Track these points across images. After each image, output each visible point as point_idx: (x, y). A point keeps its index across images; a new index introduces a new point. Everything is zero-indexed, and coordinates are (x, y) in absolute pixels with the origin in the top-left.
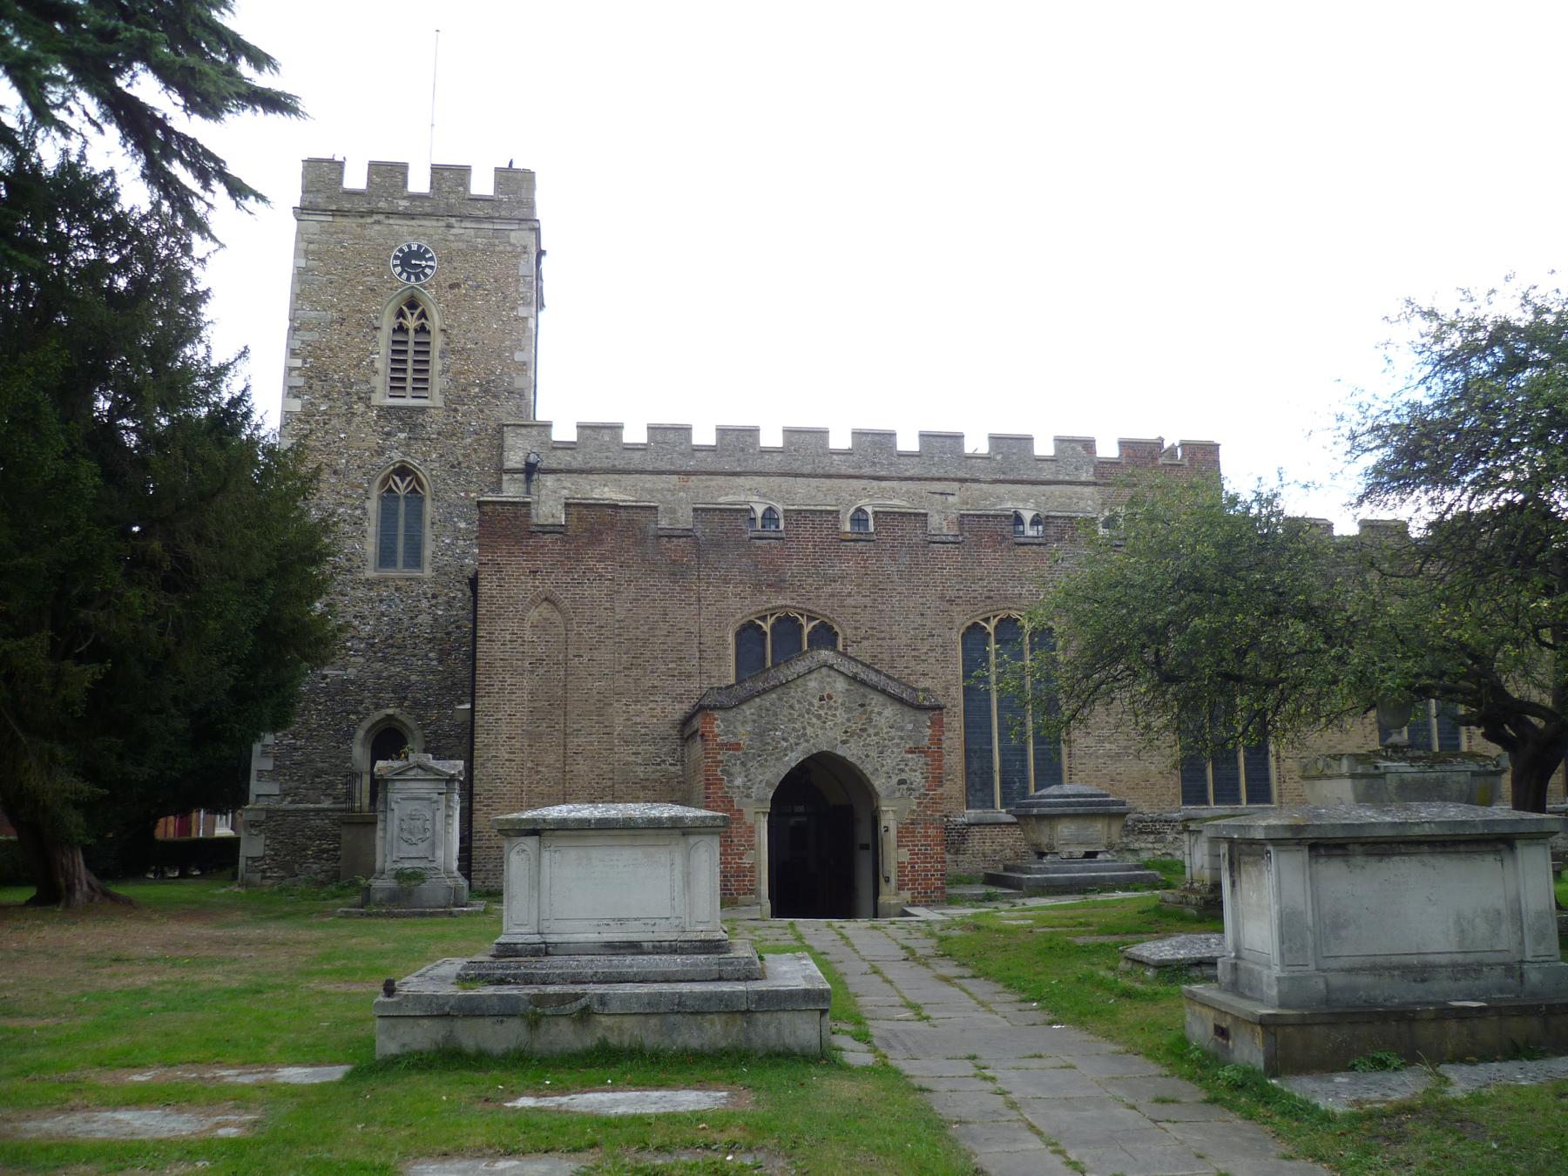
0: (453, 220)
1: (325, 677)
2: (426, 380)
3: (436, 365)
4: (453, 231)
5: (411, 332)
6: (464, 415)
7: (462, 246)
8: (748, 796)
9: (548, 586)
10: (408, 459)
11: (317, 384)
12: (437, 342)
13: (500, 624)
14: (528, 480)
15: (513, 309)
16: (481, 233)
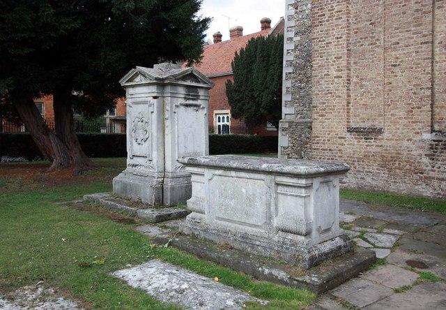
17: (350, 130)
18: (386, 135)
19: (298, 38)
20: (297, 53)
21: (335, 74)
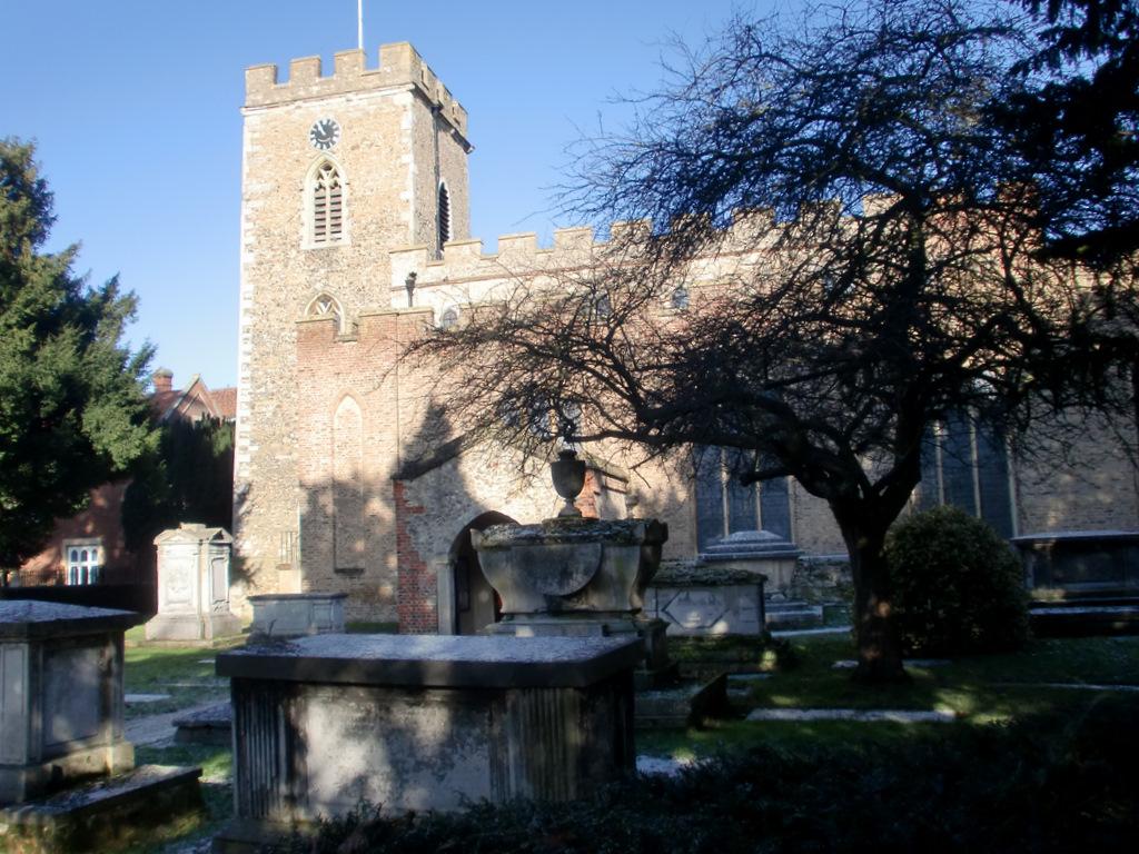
0: (350, 96)
1: (278, 461)
2: (340, 225)
3: (345, 213)
4: (351, 104)
5: (328, 189)
6: (366, 248)
7: (359, 114)
8: (430, 550)
9: (348, 385)
10: (328, 288)
11: (263, 238)
12: (345, 192)
13: (315, 417)
14: (411, 295)
15: (398, 157)
16: (373, 101)
17: (338, 571)
18: (367, 574)
19: (255, 448)
20: (255, 467)
21: (322, 520)
